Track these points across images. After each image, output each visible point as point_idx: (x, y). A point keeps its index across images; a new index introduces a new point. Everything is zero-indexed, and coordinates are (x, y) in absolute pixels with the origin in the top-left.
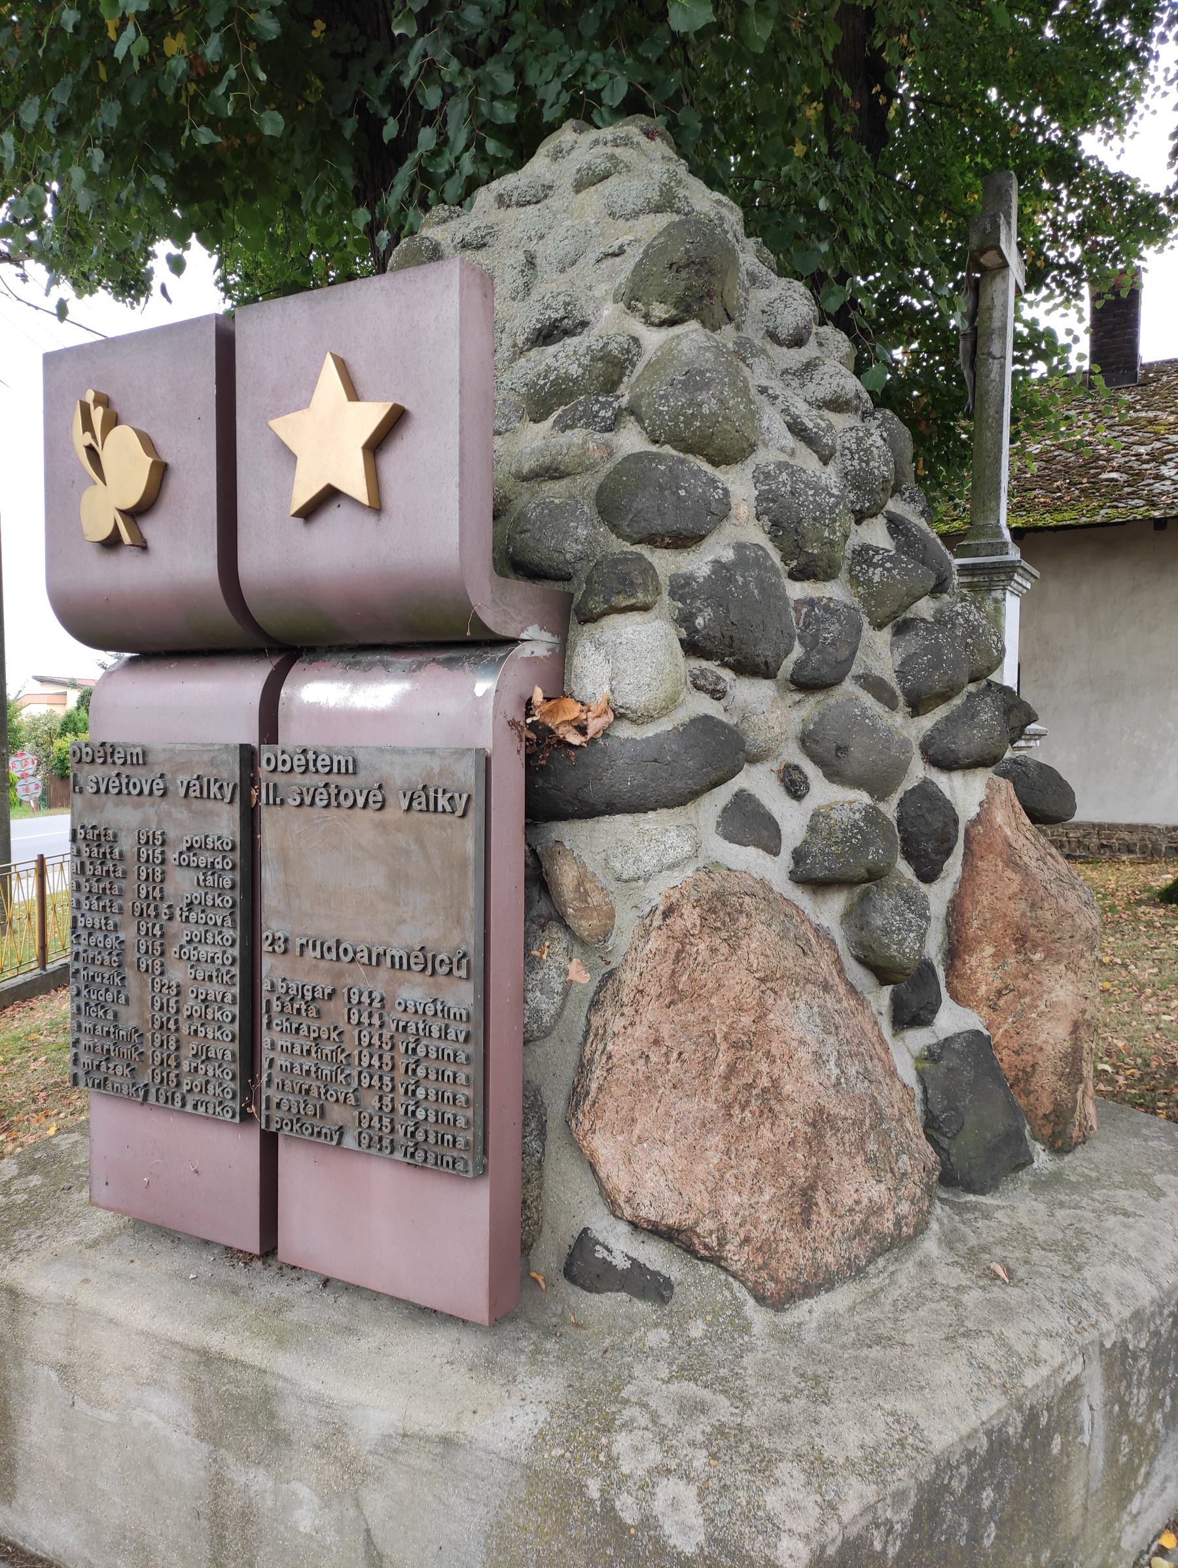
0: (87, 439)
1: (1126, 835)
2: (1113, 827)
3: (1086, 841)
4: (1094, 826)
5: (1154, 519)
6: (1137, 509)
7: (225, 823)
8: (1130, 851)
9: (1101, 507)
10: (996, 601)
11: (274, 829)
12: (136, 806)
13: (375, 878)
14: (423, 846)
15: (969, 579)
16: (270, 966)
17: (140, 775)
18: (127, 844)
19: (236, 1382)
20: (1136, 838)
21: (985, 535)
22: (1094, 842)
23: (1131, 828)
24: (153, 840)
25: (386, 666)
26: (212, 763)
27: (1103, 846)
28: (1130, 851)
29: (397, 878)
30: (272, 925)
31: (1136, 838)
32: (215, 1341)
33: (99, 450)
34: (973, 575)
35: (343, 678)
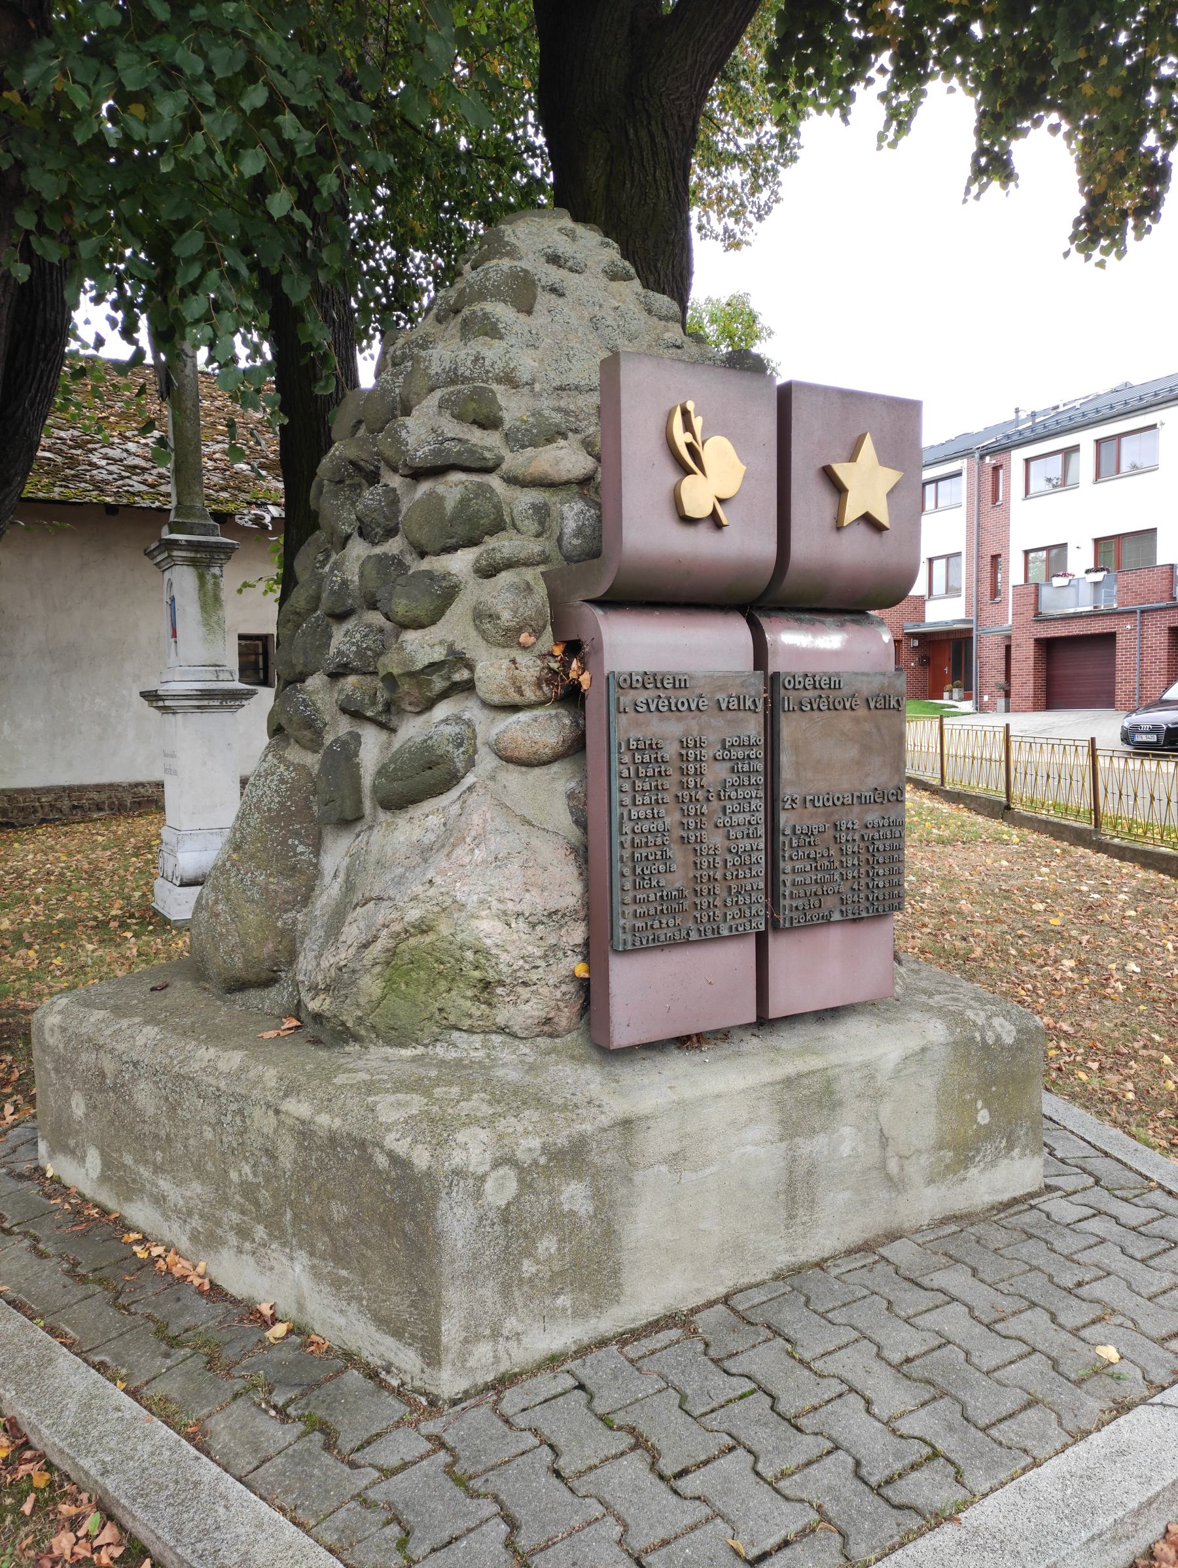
0: (688, 437)
1: (95, 795)
2: (82, 788)
3: (59, 805)
4: (64, 789)
5: (107, 505)
6: (71, 492)
7: (753, 727)
8: (100, 809)
9: (54, 485)
10: (215, 576)
11: (789, 727)
12: (679, 720)
13: (853, 752)
14: (879, 730)
15: (189, 554)
16: (786, 819)
17: (682, 695)
18: (671, 750)
19: (809, 1087)
20: (104, 796)
21: (194, 516)
22: (66, 804)
23: (99, 788)
24: (690, 747)
25: (823, 622)
26: (743, 685)
27: (75, 807)
28: (100, 809)
29: (866, 749)
30: (787, 791)
31: (104, 796)
32: (790, 1068)
33: (700, 448)
34: (196, 551)
35: (807, 630)
